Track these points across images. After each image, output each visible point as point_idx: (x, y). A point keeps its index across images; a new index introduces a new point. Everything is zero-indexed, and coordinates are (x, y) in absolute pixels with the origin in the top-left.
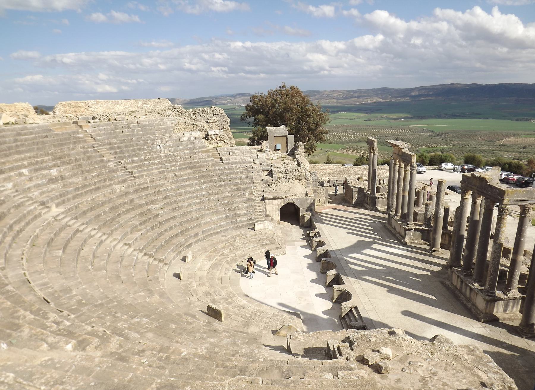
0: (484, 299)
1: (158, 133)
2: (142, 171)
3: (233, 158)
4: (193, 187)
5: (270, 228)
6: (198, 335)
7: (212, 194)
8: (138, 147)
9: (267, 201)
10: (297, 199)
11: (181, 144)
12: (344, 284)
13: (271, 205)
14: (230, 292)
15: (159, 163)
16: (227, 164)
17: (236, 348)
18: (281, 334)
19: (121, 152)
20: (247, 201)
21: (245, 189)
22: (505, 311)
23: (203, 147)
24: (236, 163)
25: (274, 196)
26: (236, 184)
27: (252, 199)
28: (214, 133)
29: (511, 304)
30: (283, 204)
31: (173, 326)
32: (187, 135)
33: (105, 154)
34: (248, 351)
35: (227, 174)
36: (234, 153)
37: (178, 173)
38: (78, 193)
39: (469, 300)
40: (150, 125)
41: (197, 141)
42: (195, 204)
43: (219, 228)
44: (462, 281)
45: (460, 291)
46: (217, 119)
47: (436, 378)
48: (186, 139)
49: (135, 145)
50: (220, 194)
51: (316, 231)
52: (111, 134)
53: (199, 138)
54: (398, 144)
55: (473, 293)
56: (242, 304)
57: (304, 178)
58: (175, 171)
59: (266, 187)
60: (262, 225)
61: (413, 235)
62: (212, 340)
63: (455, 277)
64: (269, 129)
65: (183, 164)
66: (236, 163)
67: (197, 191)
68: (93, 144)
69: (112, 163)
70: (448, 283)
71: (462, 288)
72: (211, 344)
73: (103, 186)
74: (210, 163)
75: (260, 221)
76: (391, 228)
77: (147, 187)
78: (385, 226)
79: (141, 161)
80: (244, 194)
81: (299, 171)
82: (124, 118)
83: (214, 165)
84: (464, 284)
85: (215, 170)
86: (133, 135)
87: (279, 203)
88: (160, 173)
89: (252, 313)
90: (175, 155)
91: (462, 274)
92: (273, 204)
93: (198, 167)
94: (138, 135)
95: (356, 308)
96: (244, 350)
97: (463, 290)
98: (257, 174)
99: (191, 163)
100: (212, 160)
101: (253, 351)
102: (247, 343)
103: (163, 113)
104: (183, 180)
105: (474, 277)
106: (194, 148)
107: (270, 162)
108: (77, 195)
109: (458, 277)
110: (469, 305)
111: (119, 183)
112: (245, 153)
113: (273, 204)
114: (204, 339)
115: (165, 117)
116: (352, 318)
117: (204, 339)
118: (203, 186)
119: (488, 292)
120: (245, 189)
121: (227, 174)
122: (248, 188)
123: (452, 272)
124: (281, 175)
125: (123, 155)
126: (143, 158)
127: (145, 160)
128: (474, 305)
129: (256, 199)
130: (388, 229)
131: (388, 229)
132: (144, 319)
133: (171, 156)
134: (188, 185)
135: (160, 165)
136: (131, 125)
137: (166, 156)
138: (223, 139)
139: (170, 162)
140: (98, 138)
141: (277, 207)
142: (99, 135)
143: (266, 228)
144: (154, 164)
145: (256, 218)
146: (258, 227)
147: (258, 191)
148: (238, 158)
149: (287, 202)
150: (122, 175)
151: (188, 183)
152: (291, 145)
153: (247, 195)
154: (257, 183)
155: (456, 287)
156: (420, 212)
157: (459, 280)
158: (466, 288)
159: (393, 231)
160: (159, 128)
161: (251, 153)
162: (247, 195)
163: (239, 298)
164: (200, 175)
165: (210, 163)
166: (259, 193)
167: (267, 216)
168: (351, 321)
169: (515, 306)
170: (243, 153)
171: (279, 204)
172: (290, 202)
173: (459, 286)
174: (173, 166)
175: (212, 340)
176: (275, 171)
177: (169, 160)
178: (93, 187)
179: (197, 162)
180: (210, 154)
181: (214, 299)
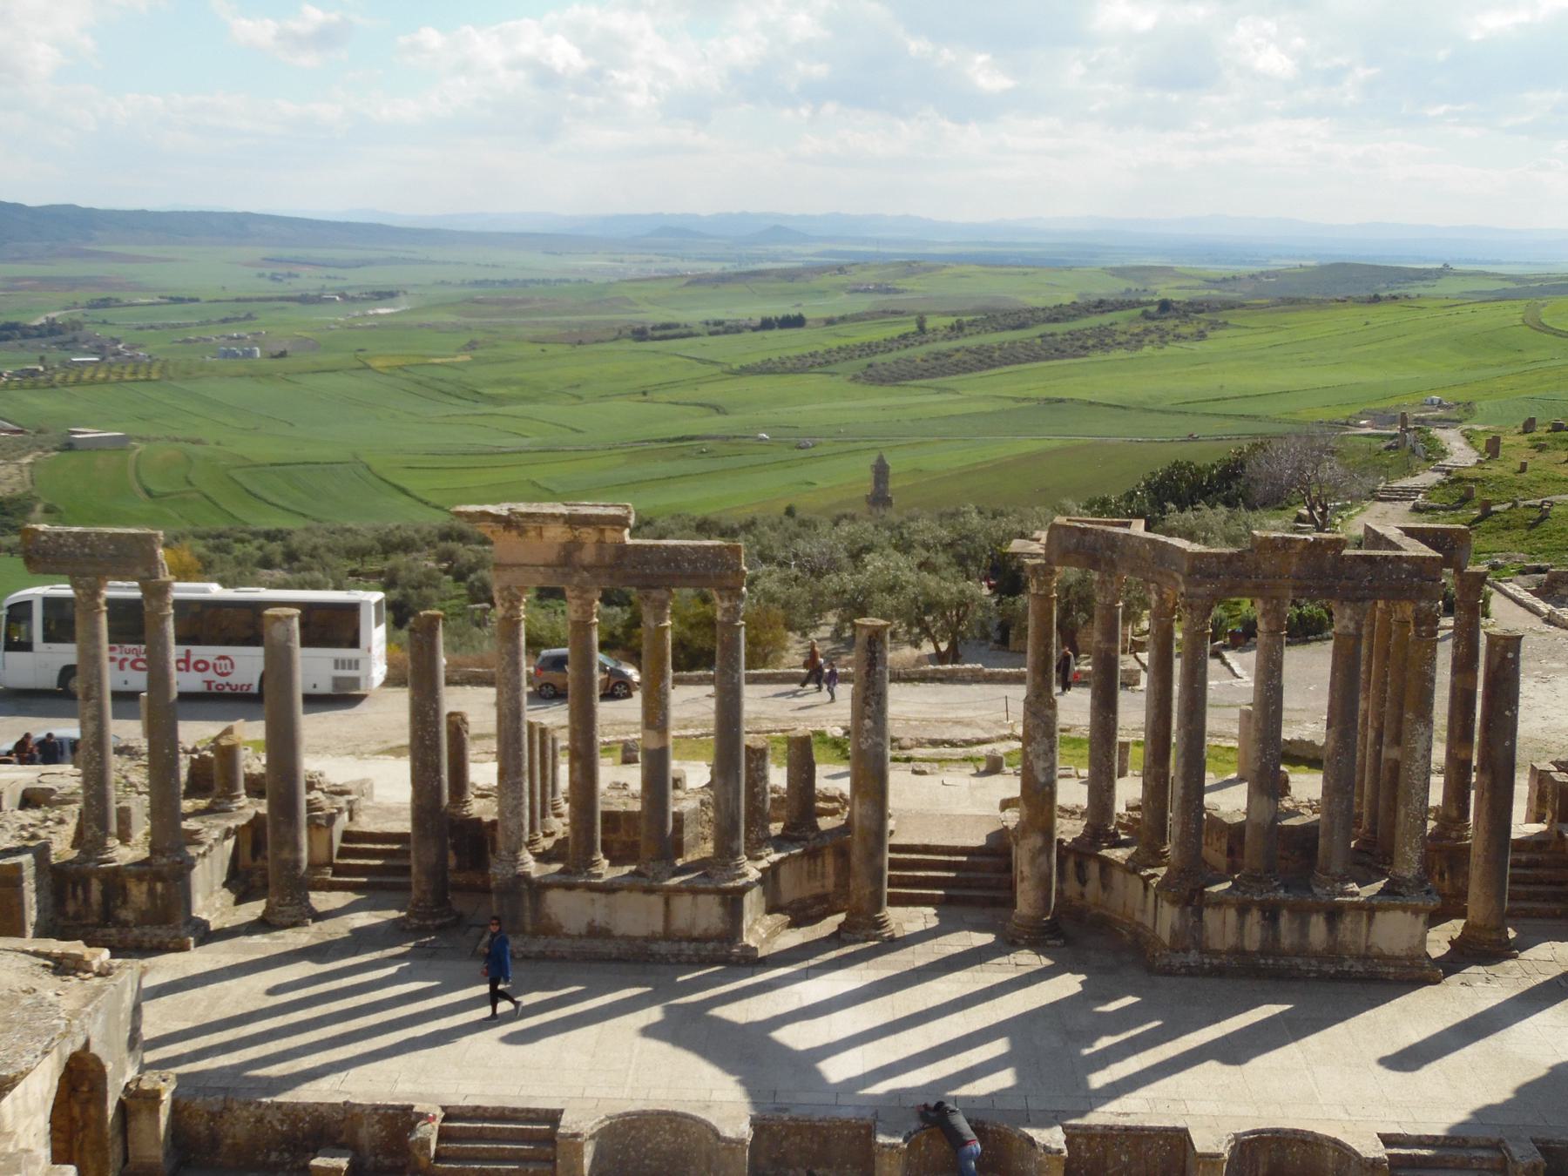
39: (1334, 952)
44: (1271, 914)
55: (1348, 922)
70: (1193, 957)
71: (1276, 939)
76: (564, 946)
84: (1284, 920)
91: (1275, 889)
97: (1287, 939)
109: (1243, 910)
123: (1199, 913)
130: (541, 957)
131: (541, 957)
155: (1238, 951)
157: (1254, 917)
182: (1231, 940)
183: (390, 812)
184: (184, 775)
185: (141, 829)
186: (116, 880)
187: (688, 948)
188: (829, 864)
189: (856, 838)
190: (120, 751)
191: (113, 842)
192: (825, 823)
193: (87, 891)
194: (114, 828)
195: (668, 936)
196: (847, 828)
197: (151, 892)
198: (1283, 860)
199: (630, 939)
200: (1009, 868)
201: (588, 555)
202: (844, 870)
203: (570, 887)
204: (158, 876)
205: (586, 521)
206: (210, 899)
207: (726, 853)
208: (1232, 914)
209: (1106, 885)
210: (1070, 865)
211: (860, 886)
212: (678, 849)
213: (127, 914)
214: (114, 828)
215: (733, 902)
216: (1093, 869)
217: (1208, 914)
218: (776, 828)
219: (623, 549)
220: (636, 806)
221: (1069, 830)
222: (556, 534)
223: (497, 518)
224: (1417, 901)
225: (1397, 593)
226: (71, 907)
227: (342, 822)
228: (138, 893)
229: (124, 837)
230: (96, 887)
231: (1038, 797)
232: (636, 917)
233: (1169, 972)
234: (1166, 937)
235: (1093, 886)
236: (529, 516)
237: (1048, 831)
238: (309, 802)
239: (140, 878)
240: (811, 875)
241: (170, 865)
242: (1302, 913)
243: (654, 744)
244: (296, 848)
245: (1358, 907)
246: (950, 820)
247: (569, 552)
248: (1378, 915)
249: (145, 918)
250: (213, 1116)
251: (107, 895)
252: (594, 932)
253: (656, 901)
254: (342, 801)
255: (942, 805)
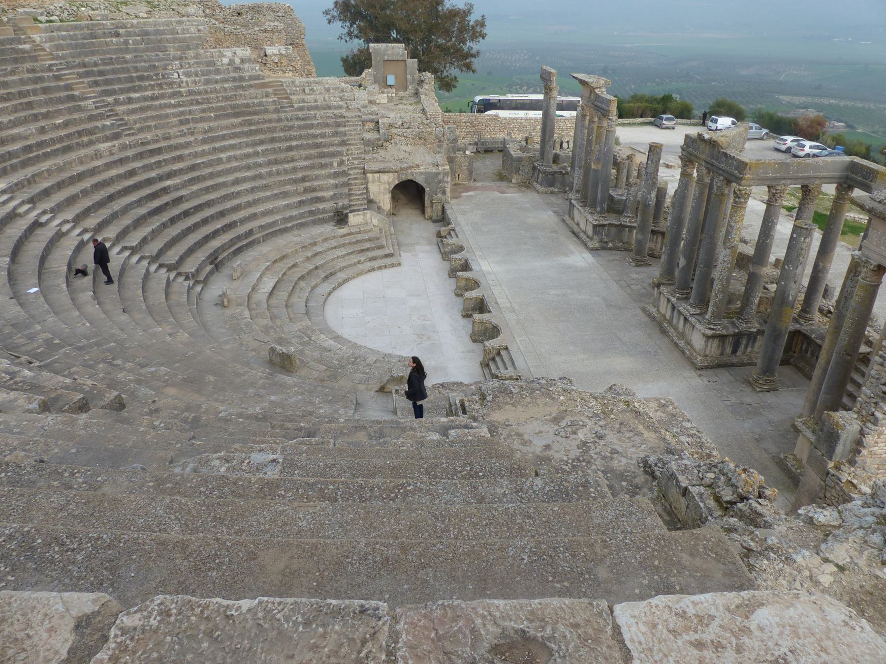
0: (704, 335)
1: (174, 47)
2: (148, 118)
3: (310, 98)
4: (240, 148)
5: (375, 222)
6: (251, 391)
7: (276, 162)
8: (139, 74)
9: (369, 176)
10: (421, 173)
11: (218, 72)
12: (489, 312)
13: (377, 184)
14: (307, 327)
15: (179, 105)
16: (301, 109)
17: (310, 408)
18: (386, 390)
19: (107, 82)
20: (336, 175)
21: (333, 155)
22: (734, 352)
23: (258, 77)
24: (316, 108)
25: (382, 166)
26: (317, 146)
27: (344, 173)
28: (275, 51)
29: (744, 342)
30: (397, 182)
31: (211, 378)
32: (228, 53)
33: (76, 84)
34: (329, 411)
35: (300, 128)
36: (312, 90)
37: (213, 124)
38: (31, 155)
39: (682, 335)
40: (157, 32)
41: (247, 65)
42: (245, 180)
43: (289, 222)
44: (673, 308)
45: (670, 322)
46: (281, 26)
47: (602, 443)
48: (226, 61)
49: (132, 70)
50: (288, 162)
51: (450, 226)
52: (83, 46)
53: (249, 60)
54: (591, 80)
56: (326, 345)
57: (433, 136)
58: (209, 119)
59: (366, 152)
60: (362, 217)
61: (607, 235)
62: (273, 398)
63: (663, 302)
64: (374, 48)
65: (222, 108)
66: (316, 108)
67: (247, 156)
68: (51, 65)
69: (91, 101)
70: (653, 310)
72: (271, 402)
73: (77, 144)
74: (271, 107)
75: (359, 210)
77: (160, 149)
78: (564, 221)
79: (145, 99)
80: (331, 165)
82: (107, 16)
83: (277, 111)
84: (676, 312)
85: (279, 120)
86: (127, 51)
87: (391, 180)
88: (182, 123)
89: (342, 358)
90: (206, 92)
92: (380, 182)
93: (250, 114)
94: (136, 50)
95: (506, 348)
96: (322, 411)
97: (675, 321)
98: (352, 128)
99: (237, 106)
100: (274, 101)
101: (336, 411)
102: (330, 402)
103: (182, 10)
104: (224, 138)
105: (691, 301)
106: (241, 79)
107: (375, 108)
108: (30, 159)
109: (669, 300)
110: (682, 344)
111: (107, 139)
112: (331, 91)
113: (380, 182)
114: (261, 397)
115: (185, 19)
116: (500, 365)
117: (261, 397)
118: (260, 149)
119: (710, 323)
120: (333, 155)
121: (300, 128)
122: (339, 154)
123: (660, 293)
124: (394, 130)
125: (110, 88)
126: (149, 93)
127: (153, 98)
128: (688, 343)
129: (351, 172)
130: (567, 225)
132: (162, 368)
133: (199, 93)
134: (232, 147)
135: (181, 109)
136: (121, 31)
137: (190, 93)
138: (293, 64)
139: (198, 103)
140: (60, 53)
141: (387, 186)
142: (59, 47)
143: (369, 221)
144: (170, 106)
145: (350, 206)
146: (353, 219)
147: (355, 159)
148: (320, 98)
149: (404, 178)
150: (112, 124)
151: (232, 142)
152: (413, 77)
153: (335, 164)
154: (353, 144)
155: (665, 317)
156: (619, 197)
157: (670, 306)
158: (679, 318)
159: (576, 229)
160: (176, 39)
161: (343, 91)
162: (335, 164)
163: (323, 336)
164: (254, 128)
165: (271, 107)
166: (356, 162)
167: (370, 201)
168: (498, 369)
169: (750, 344)
170: (328, 90)
171: (391, 180)
172: (410, 178)
174: (204, 111)
175: (273, 398)
176: (383, 124)
177: (197, 101)
178: (58, 146)
179: (248, 105)
180: (270, 90)
181: (281, 338)
195: (585, 232)
219: (597, 96)
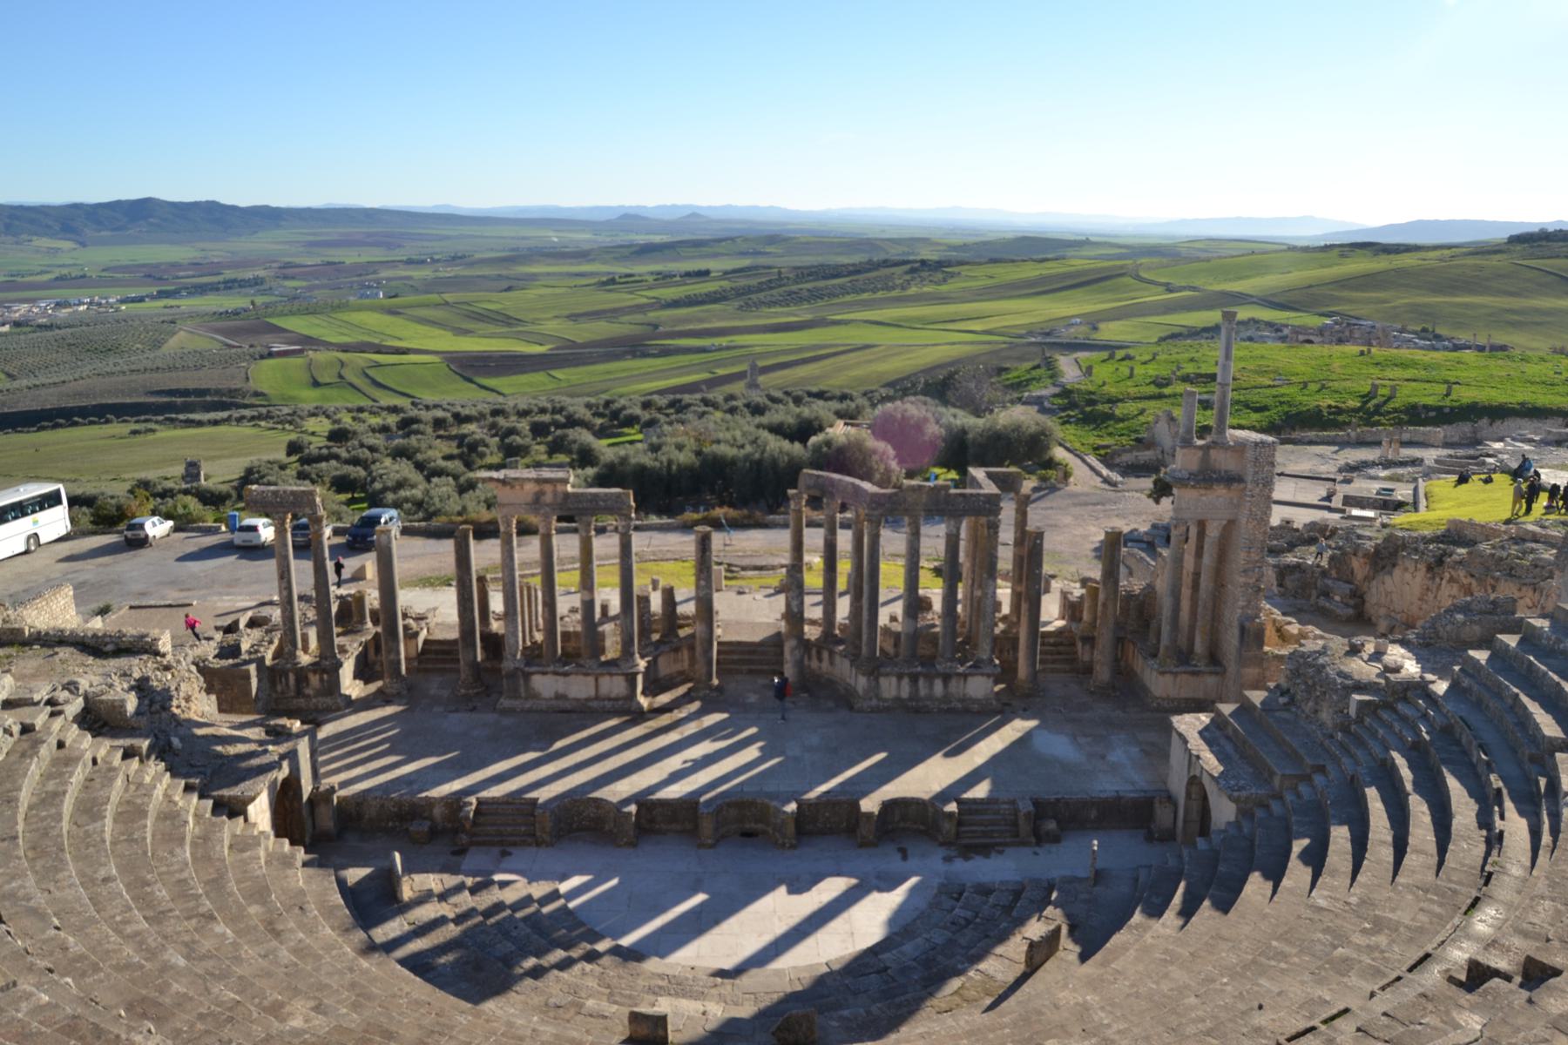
44: (914, 679)
55: (953, 683)
70: (874, 702)
71: (917, 690)
81: (167, 668)
84: (921, 682)
97: (923, 692)
109: (900, 677)
123: (877, 679)
128: (963, 700)
155: (898, 699)
157: (906, 681)
158: (931, 686)
173: (905, 691)
182: (894, 693)
183: (450, 627)
184: (334, 609)
185: (313, 643)
186: (302, 674)
187: (608, 704)
188: (685, 654)
189: (698, 643)
190: (301, 598)
191: (300, 653)
192: (682, 633)
193: (287, 679)
194: (300, 645)
196: (693, 636)
197: (321, 680)
198: (920, 651)
199: (577, 700)
200: (782, 653)
201: (548, 498)
202: (693, 660)
203: (544, 673)
204: (324, 671)
205: (547, 481)
206: (351, 686)
207: (627, 653)
208: (894, 680)
209: (832, 663)
210: (814, 652)
211: (700, 668)
212: (603, 651)
213: (309, 691)
214: (300, 645)
215: (631, 679)
216: (825, 655)
217: (882, 680)
218: (656, 637)
219: (567, 495)
220: (579, 628)
221: (812, 633)
222: (530, 488)
223: (498, 480)
224: (988, 670)
225: (977, 512)
226: (279, 688)
227: (423, 635)
228: (314, 680)
229: (305, 649)
230: (292, 677)
231: (794, 617)
232: (579, 687)
233: (861, 711)
234: (860, 690)
235: (825, 665)
236: (516, 479)
237: (800, 635)
238: (406, 628)
239: (315, 672)
240: (676, 661)
241: (328, 666)
242: (930, 678)
243: (587, 598)
244: (398, 653)
245: (959, 675)
246: (754, 626)
247: (538, 496)
248: (970, 679)
249: (319, 693)
250: (358, 804)
251: (298, 681)
252: (558, 697)
253: (591, 680)
254: (423, 623)
255: (749, 613)
